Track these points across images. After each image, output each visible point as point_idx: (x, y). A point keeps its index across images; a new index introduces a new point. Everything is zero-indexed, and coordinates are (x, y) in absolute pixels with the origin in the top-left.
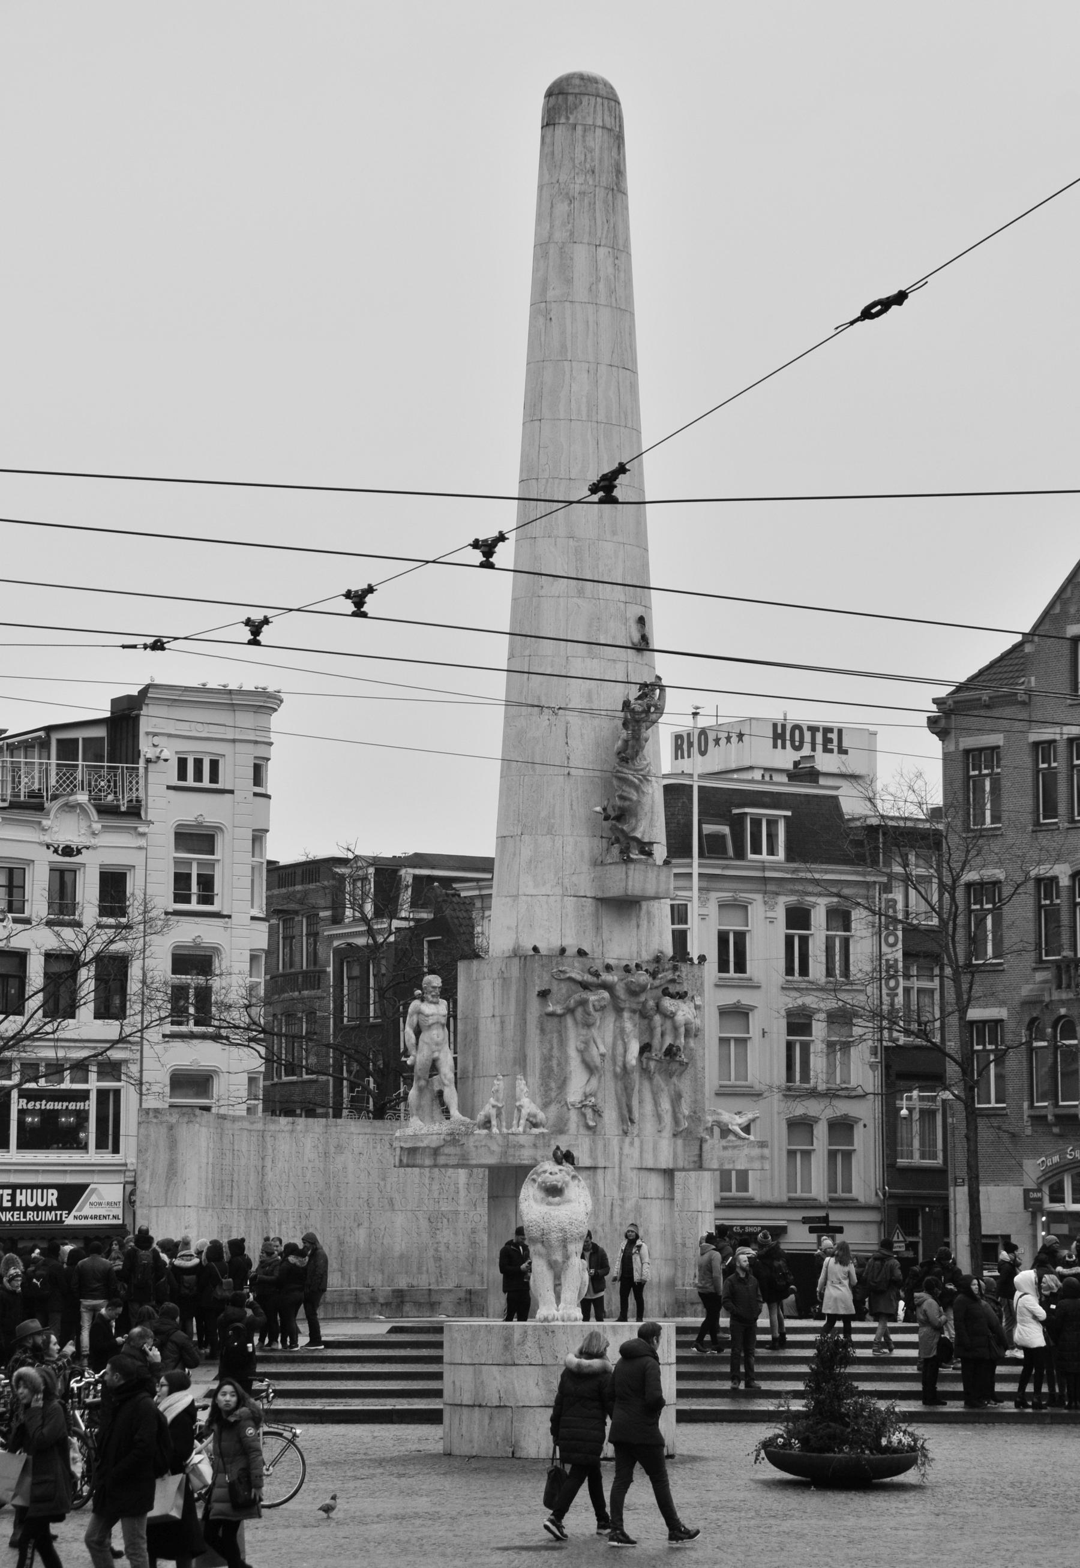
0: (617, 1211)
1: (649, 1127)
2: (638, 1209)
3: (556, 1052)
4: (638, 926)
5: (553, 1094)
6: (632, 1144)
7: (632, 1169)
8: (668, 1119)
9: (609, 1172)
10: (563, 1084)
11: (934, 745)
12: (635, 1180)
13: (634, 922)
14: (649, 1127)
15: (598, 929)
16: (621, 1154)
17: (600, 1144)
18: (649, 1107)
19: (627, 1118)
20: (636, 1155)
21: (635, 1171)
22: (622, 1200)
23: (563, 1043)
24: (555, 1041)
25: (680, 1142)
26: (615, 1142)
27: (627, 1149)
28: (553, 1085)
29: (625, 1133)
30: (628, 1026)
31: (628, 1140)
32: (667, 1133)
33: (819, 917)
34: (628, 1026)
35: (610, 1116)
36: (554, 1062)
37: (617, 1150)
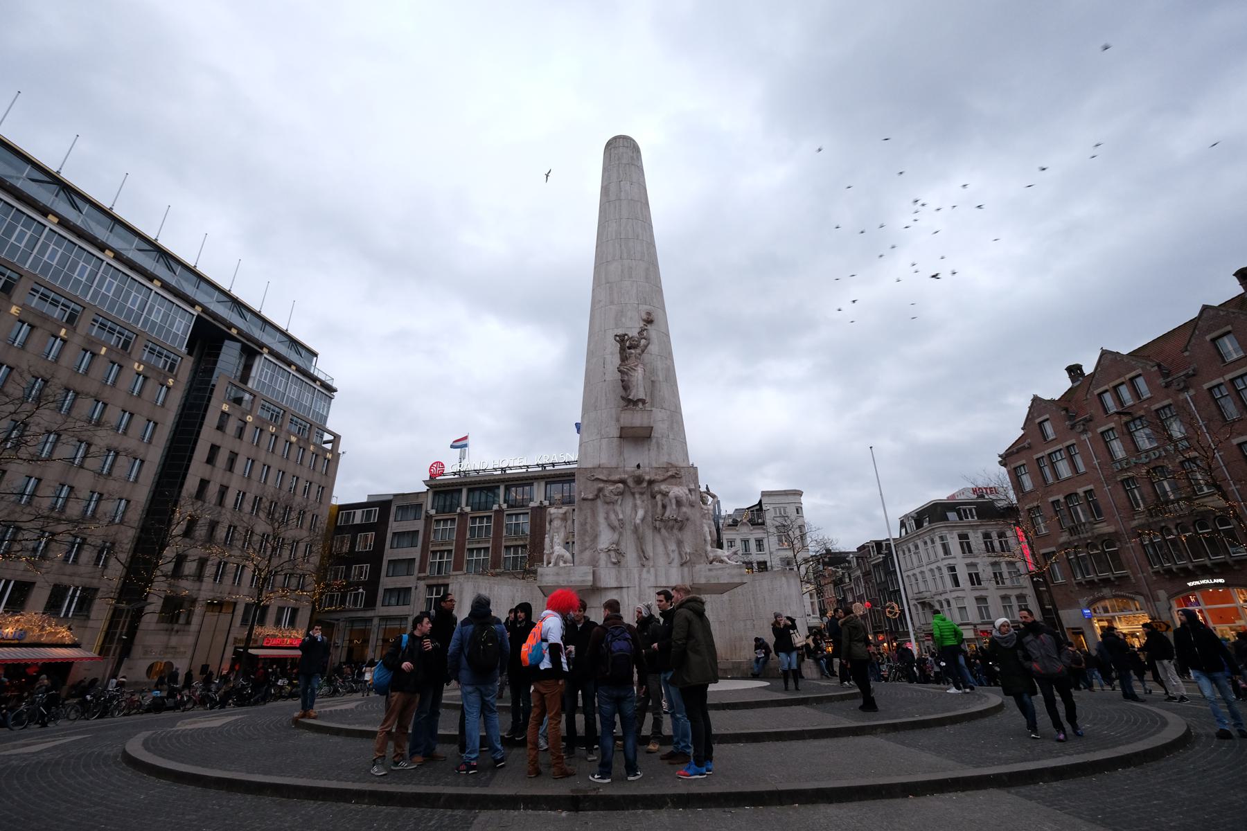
1: (662, 561)
3: (589, 520)
6: (648, 572)
8: (675, 556)
9: (631, 591)
10: (595, 538)
11: (1004, 469)
13: (646, 448)
14: (662, 561)
15: (621, 453)
16: (640, 578)
17: (624, 573)
18: (660, 549)
19: (643, 556)
20: (652, 578)
23: (594, 515)
24: (589, 515)
25: (686, 569)
27: (645, 575)
30: (639, 502)
32: (676, 562)
33: (994, 535)
34: (639, 502)
35: (631, 556)
36: (588, 527)
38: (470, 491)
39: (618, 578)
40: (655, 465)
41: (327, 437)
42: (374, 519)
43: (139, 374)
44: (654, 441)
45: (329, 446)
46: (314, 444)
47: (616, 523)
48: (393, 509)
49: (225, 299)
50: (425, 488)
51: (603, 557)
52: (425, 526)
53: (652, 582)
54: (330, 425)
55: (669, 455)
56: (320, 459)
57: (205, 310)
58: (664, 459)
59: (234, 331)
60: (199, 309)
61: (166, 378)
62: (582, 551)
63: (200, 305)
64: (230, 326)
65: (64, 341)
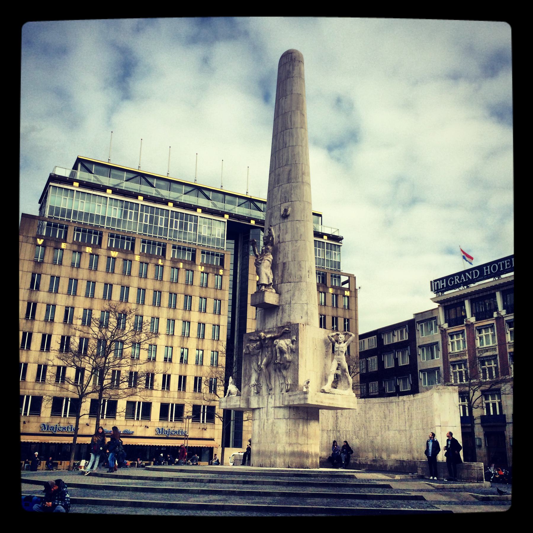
0: (266, 424)
2: (273, 424)
3: (248, 367)
4: (277, 315)
5: (246, 382)
6: (271, 398)
7: (271, 408)
10: (250, 377)
12: (273, 412)
13: (276, 314)
18: (277, 383)
20: (273, 402)
21: (273, 408)
22: (267, 420)
26: (266, 398)
27: (270, 400)
28: (247, 379)
29: (269, 394)
31: (270, 396)
37: (266, 400)
38: (472, 302)
39: (258, 404)
40: (279, 325)
41: (344, 279)
42: (406, 337)
43: (202, 272)
44: (281, 308)
45: (346, 286)
46: (332, 287)
47: (256, 367)
48: (418, 327)
49: (244, 201)
50: (436, 305)
51: (252, 388)
52: (443, 340)
53: (272, 405)
54: (344, 269)
55: (289, 316)
56: (340, 297)
57: (231, 215)
58: (286, 320)
59: (253, 222)
60: (227, 216)
61: (218, 269)
62: (244, 387)
63: (227, 213)
64: (249, 219)
65: (162, 266)
